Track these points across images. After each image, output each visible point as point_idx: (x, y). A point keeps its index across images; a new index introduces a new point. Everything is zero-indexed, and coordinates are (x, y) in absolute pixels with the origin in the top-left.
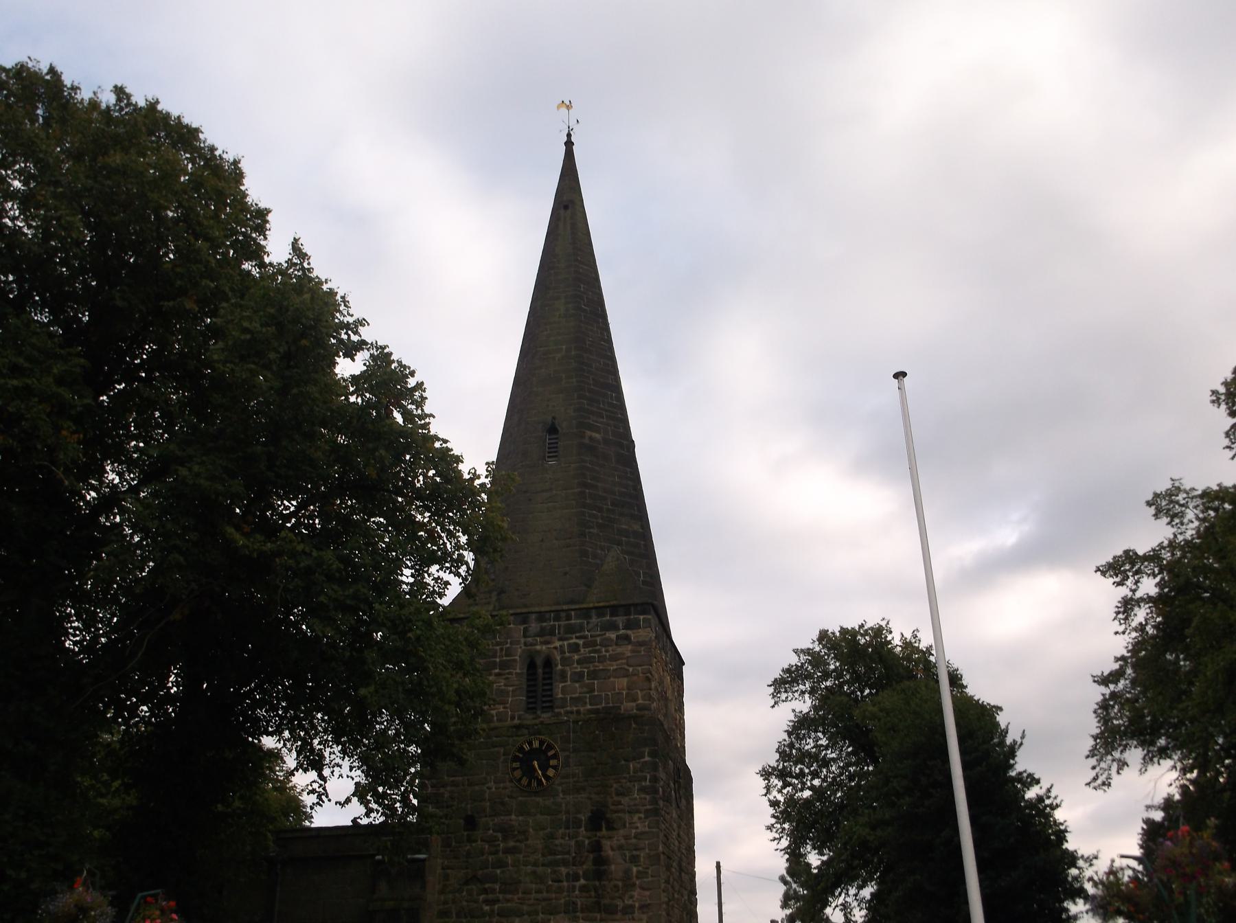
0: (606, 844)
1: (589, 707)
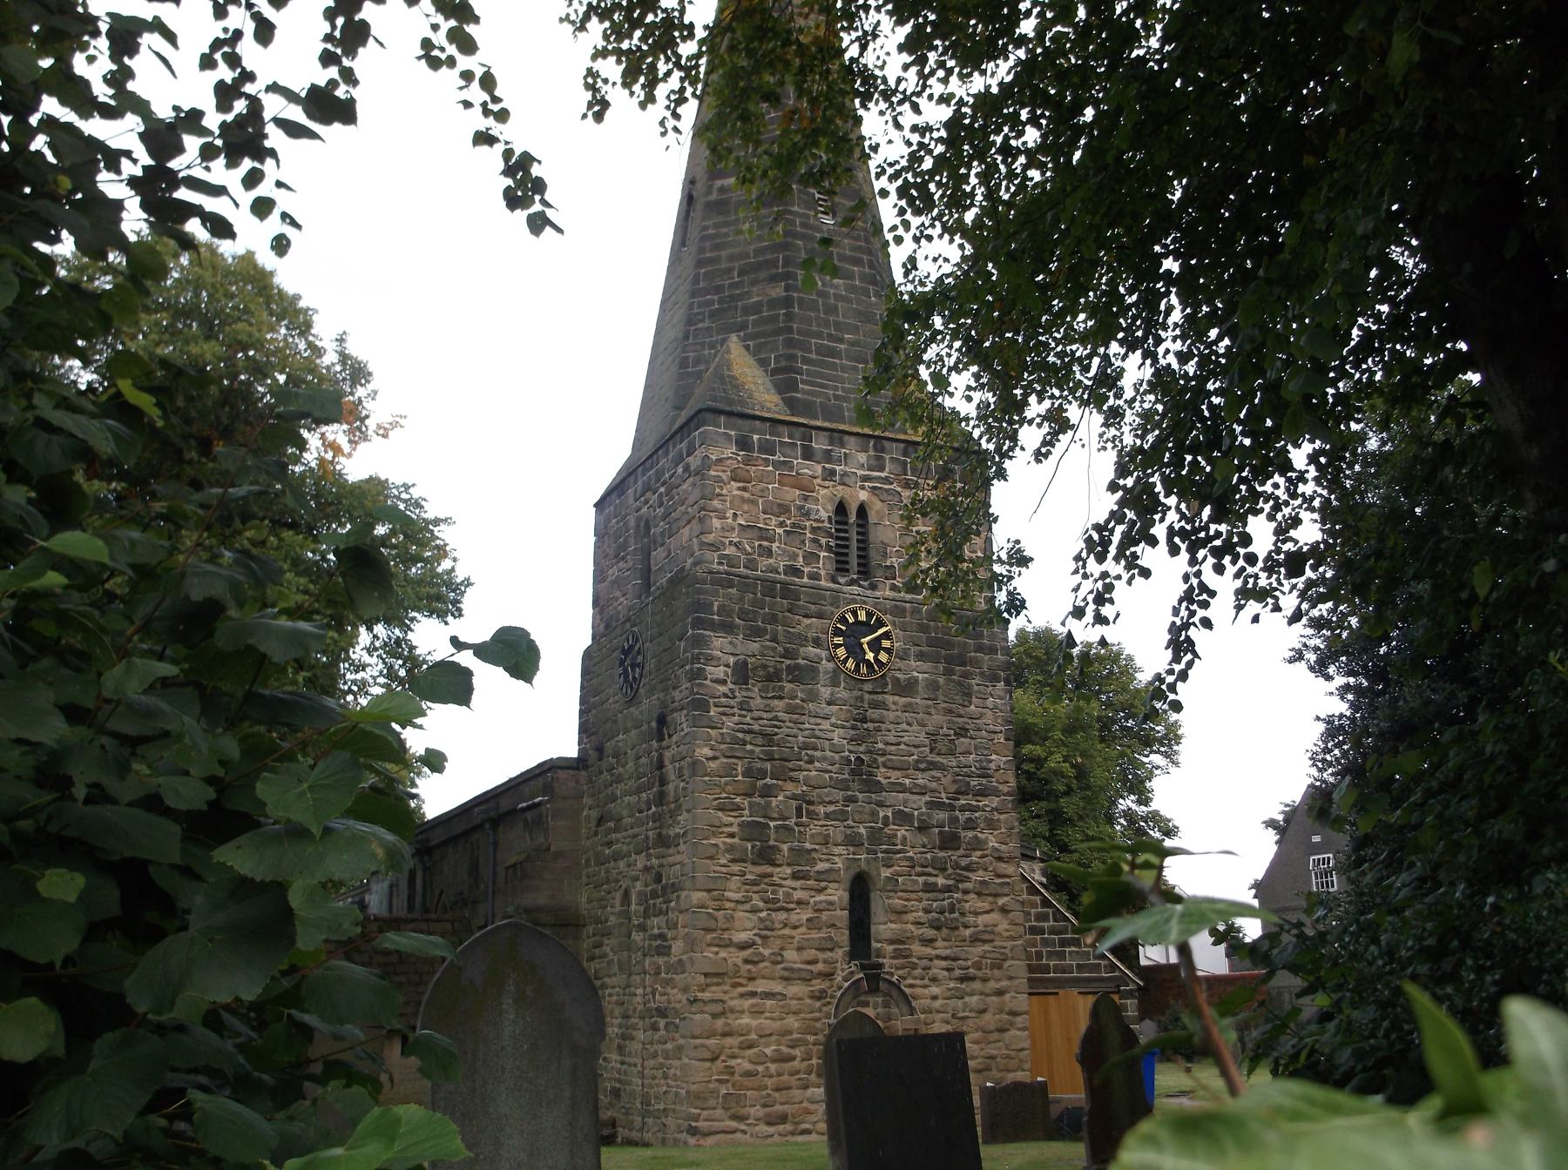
0: (668, 755)
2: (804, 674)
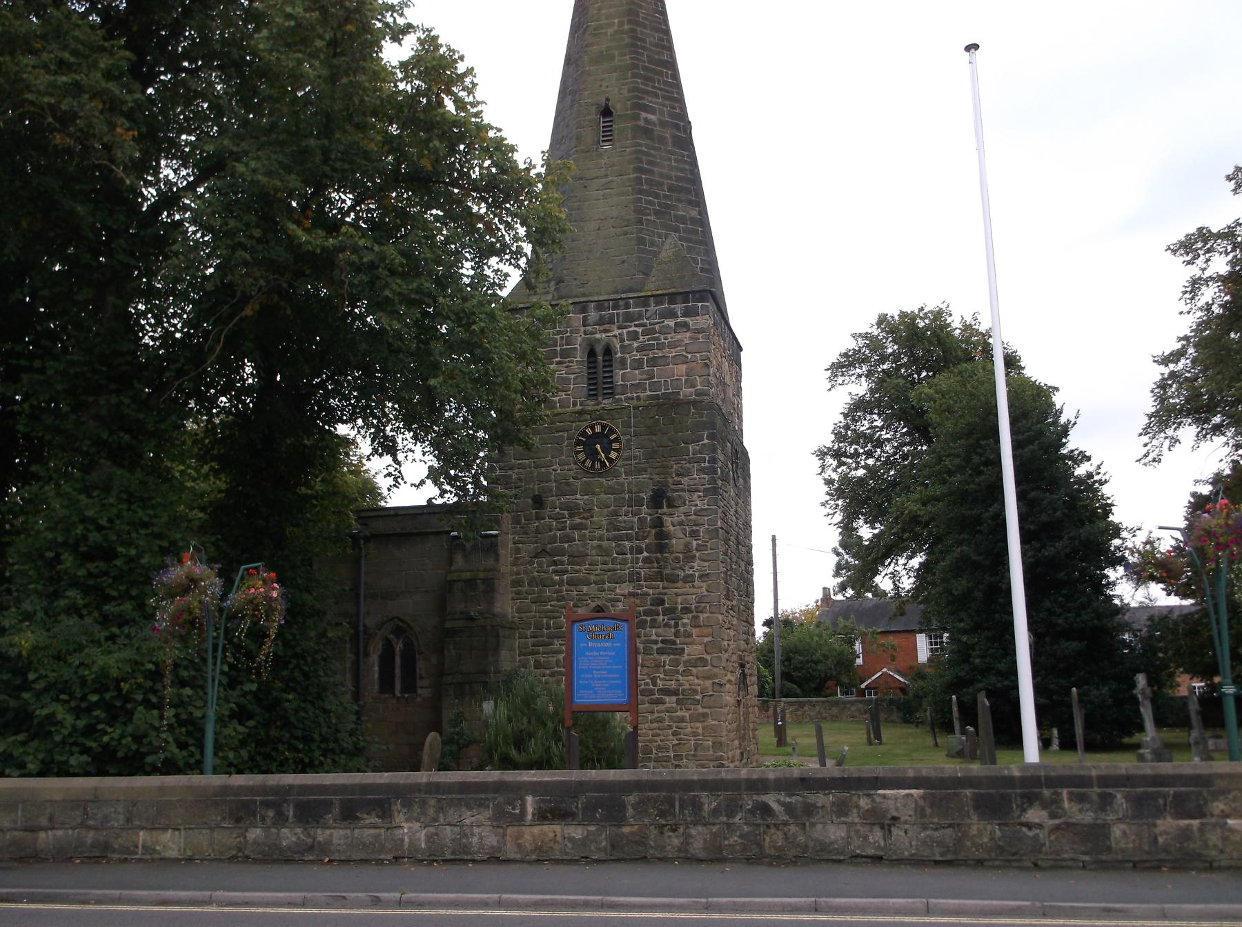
0: (667, 521)
1: (649, 393)
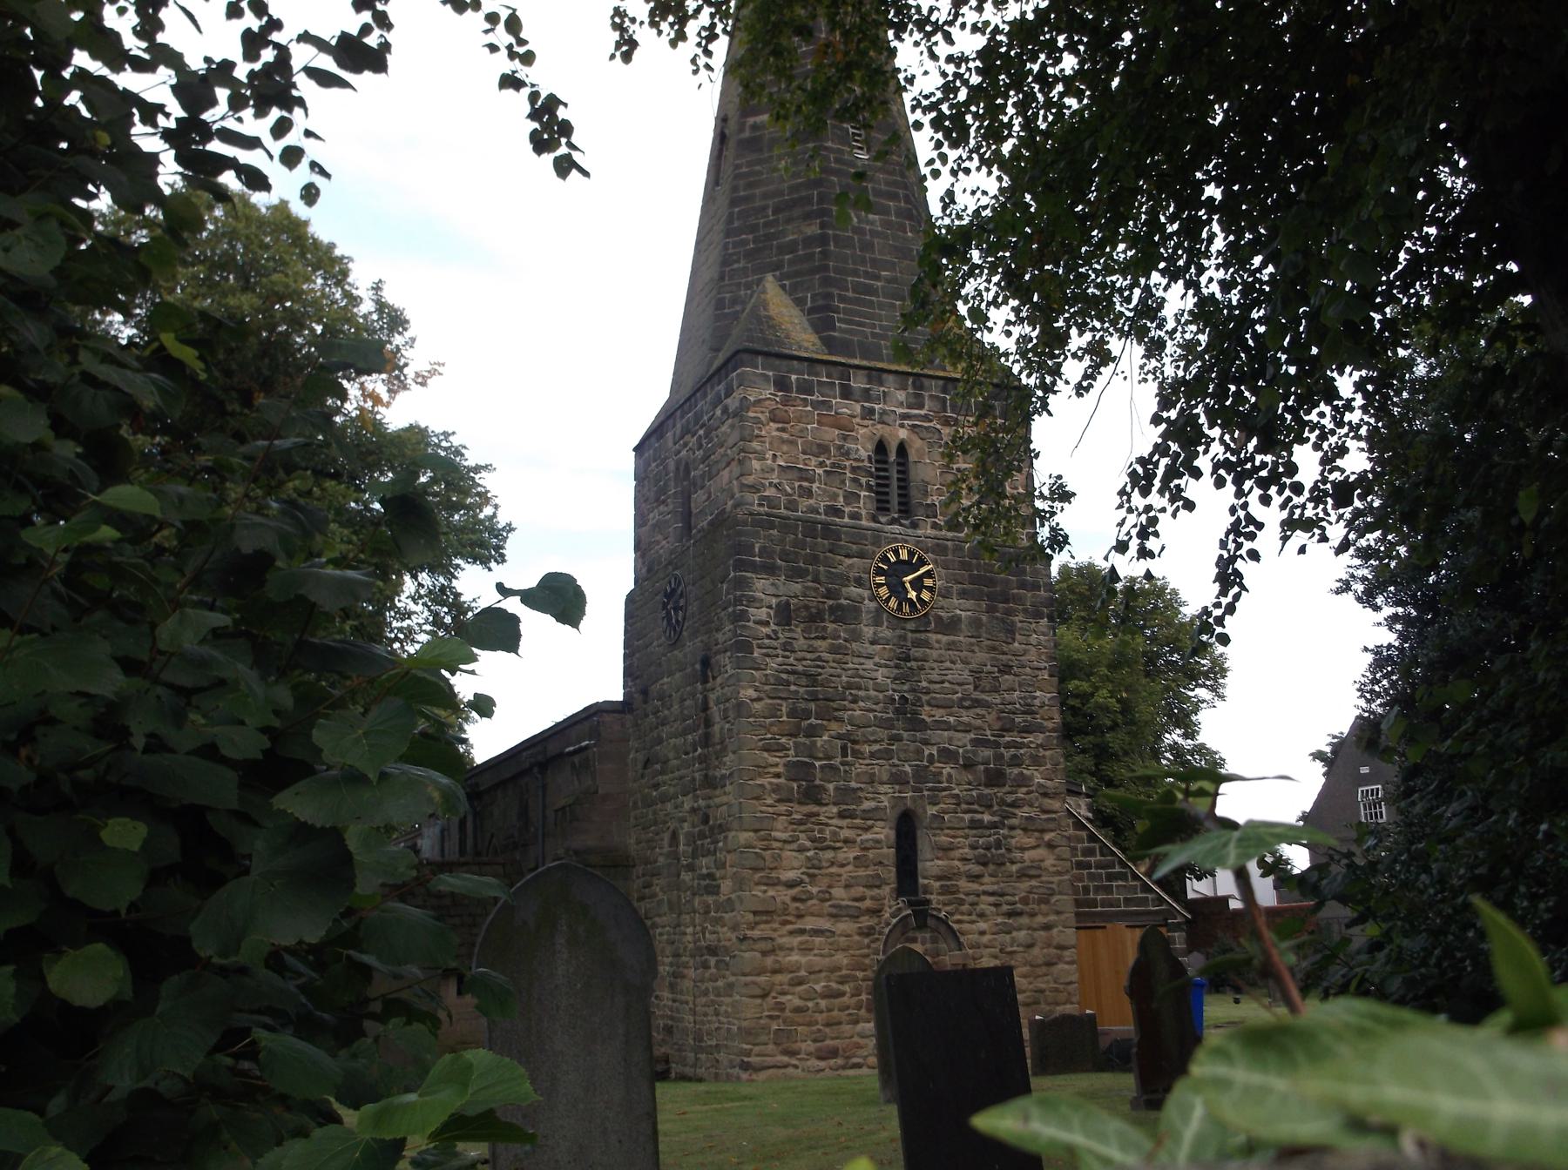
0: (712, 696)
2: (846, 615)
